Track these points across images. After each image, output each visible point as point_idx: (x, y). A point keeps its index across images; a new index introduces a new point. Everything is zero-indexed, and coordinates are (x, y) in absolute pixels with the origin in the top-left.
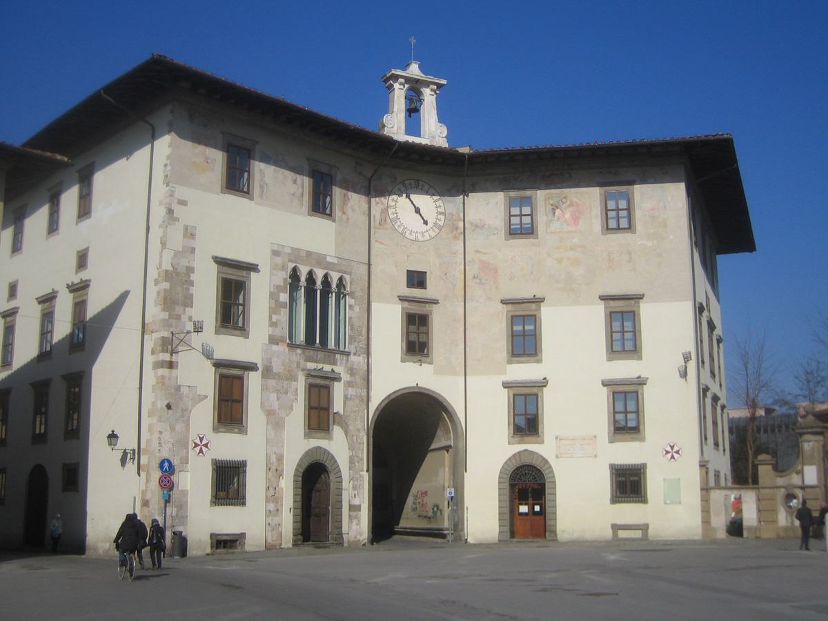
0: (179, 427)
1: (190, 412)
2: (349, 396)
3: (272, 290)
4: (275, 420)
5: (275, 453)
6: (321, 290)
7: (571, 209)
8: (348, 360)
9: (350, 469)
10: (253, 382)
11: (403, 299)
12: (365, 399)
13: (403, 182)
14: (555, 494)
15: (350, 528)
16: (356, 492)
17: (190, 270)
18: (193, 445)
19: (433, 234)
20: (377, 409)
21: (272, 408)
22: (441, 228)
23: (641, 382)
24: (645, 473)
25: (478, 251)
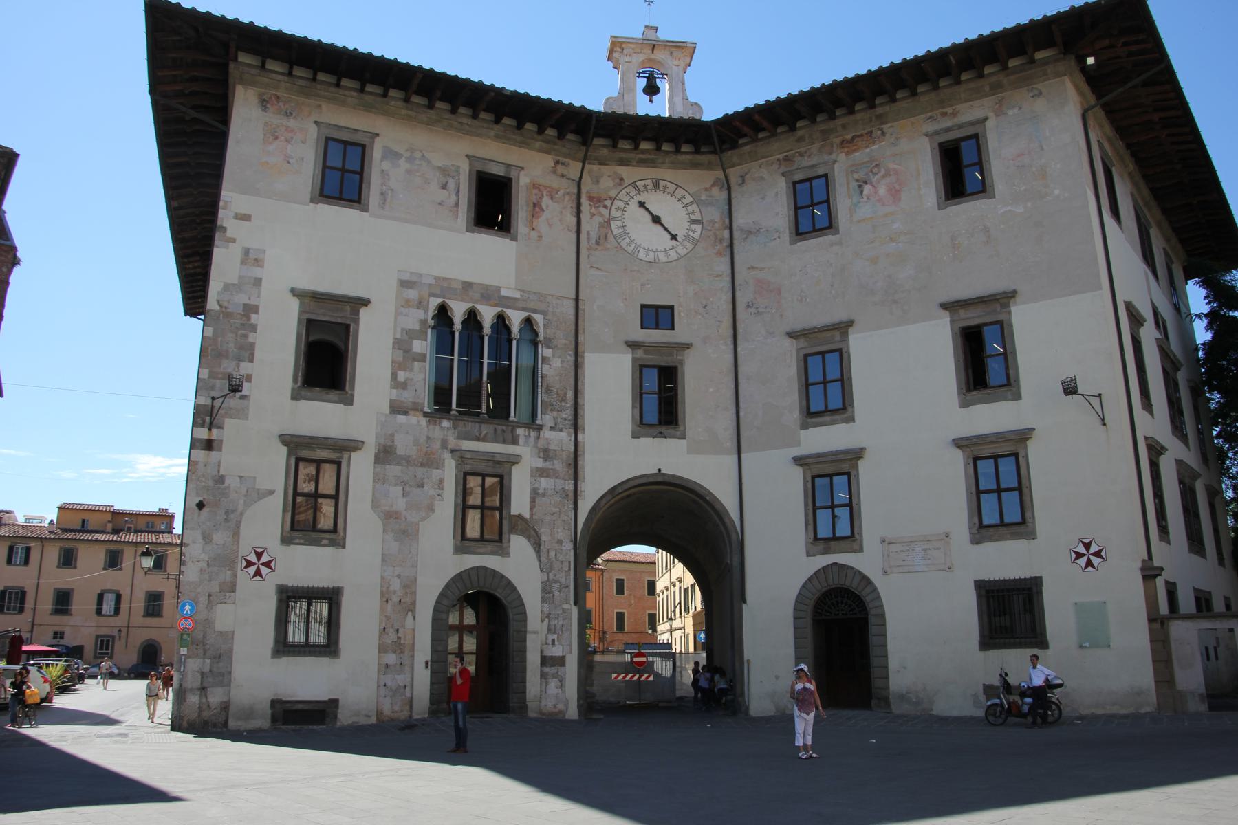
0: (220, 537)
1: (242, 514)
2: (541, 491)
3: (398, 336)
4: (400, 528)
5: (399, 576)
6: (490, 338)
7: (888, 180)
8: (539, 437)
9: (543, 600)
10: (360, 468)
11: (633, 345)
12: (571, 494)
13: (634, 185)
14: (885, 635)
15: (543, 693)
16: (555, 637)
17: (251, 309)
18: (244, 564)
19: (683, 252)
20: (594, 510)
21: (394, 508)
22: (695, 242)
23: (1023, 436)
24: (1040, 593)
25: (753, 268)
